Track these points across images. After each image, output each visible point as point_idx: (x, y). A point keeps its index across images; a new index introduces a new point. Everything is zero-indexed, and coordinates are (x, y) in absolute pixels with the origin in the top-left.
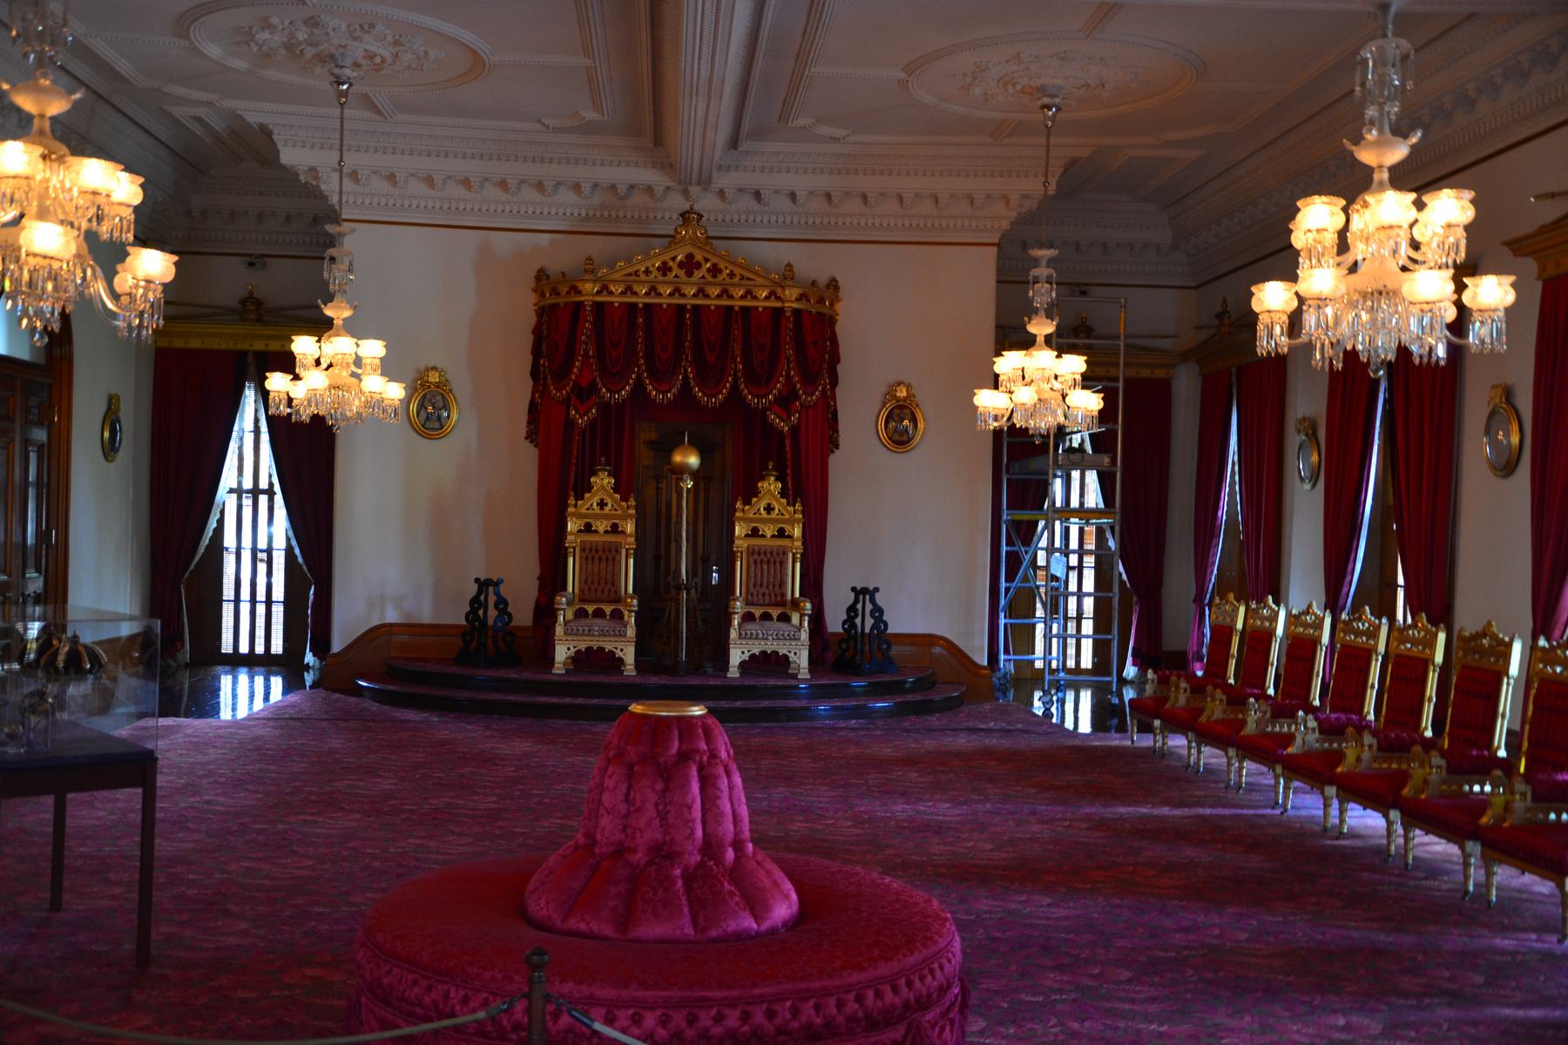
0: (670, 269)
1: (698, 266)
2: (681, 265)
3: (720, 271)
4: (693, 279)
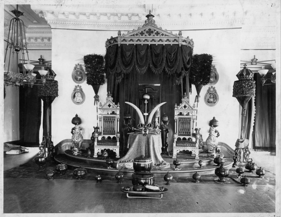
0: (144, 34)
1: (152, 32)
2: (147, 32)
3: (159, 34)
4: (151, 36)
